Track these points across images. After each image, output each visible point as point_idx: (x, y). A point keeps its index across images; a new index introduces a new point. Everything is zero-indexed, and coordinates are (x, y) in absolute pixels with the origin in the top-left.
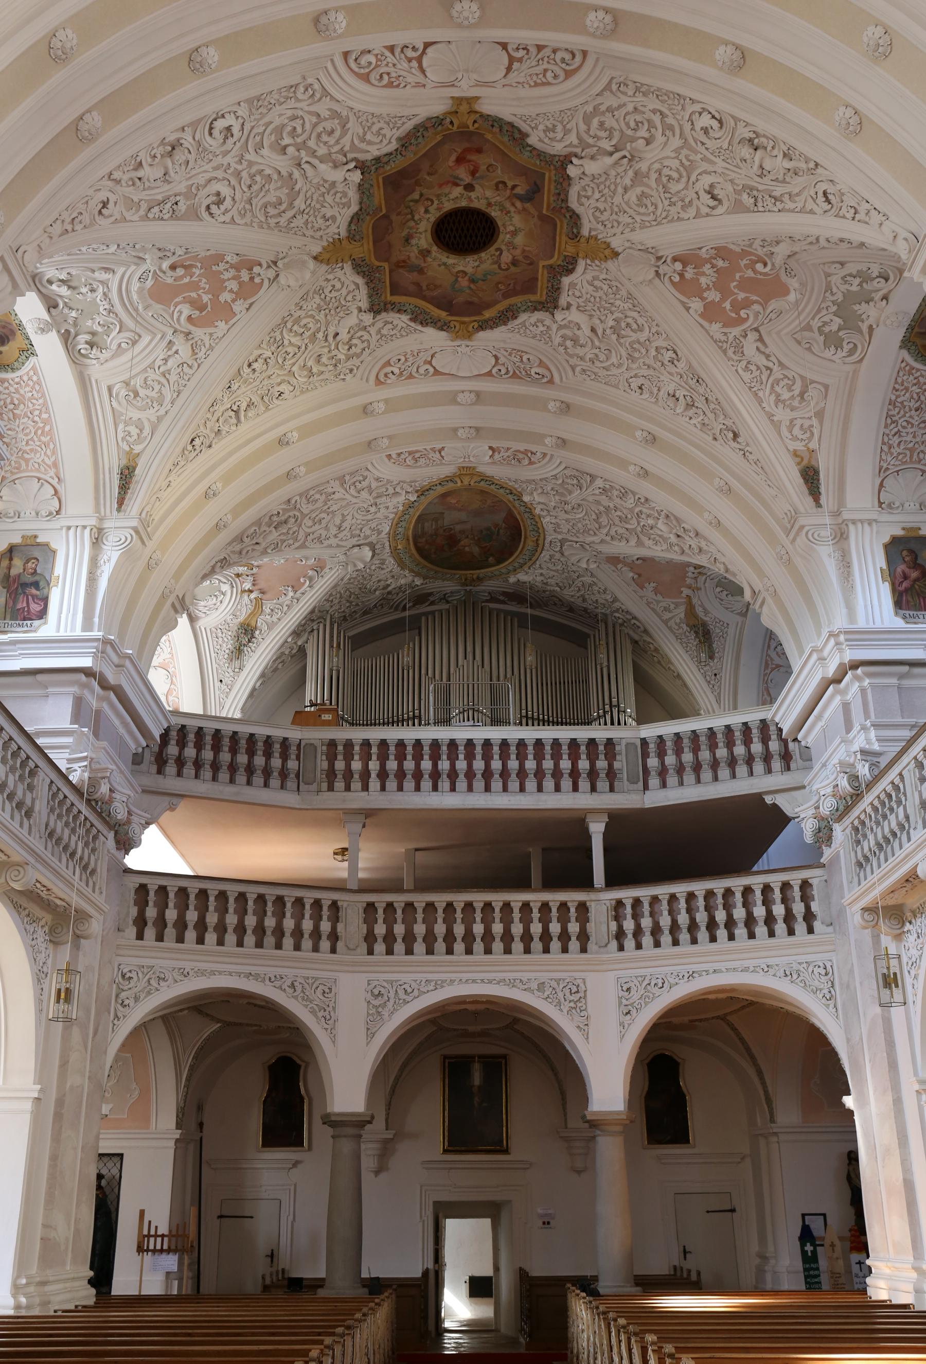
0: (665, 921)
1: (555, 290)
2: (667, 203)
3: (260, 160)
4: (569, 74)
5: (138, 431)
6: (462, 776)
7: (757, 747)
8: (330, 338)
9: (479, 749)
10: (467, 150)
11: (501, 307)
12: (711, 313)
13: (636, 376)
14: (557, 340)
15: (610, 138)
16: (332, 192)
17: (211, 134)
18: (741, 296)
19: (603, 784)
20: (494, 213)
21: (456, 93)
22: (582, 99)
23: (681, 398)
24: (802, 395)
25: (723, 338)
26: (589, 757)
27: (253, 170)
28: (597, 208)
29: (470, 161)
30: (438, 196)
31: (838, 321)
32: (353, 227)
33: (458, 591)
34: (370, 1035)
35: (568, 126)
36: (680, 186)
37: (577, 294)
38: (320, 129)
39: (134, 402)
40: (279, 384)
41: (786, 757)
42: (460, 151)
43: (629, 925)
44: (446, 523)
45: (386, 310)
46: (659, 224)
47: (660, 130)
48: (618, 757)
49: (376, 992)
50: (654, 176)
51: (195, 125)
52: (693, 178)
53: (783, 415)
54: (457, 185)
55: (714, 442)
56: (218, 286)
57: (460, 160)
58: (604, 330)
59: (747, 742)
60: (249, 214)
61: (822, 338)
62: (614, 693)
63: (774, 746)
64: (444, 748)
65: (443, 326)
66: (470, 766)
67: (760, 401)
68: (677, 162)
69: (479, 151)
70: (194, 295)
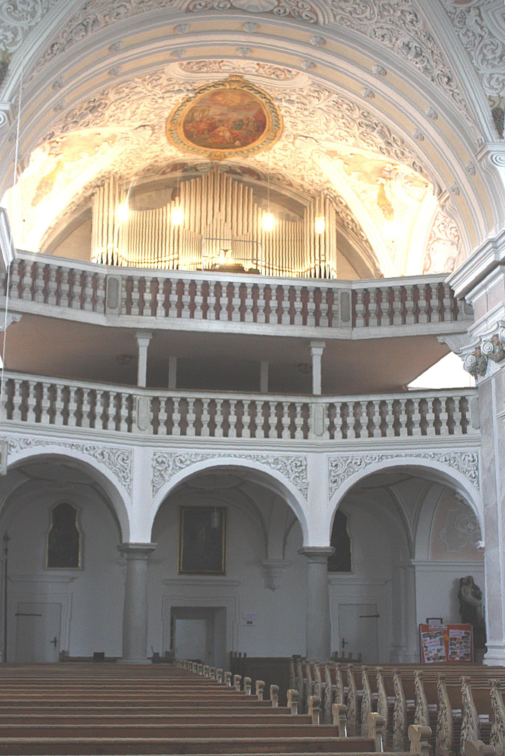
0: (364, 420)
5: (12, 36)
6: (224, 309)
7: (434, 302)
9: (237, 290)
13: (382, 28)
19: (324, 321)
23: (413, 49)
26: (315, 301)
33: (207, 164)
34: (155, 491)
39: (13, 14)
40: (118, 7)
41: (455, 311)
43: (338, 421)
44: (211, 113)
48: (335, 302)
49: (160, 460)
55: (432, 83)
59: (428, 298)
62: (322, 252)
63: (447, 302)
64: (212, 288)
66: (230, 302)
67: (471, 58)
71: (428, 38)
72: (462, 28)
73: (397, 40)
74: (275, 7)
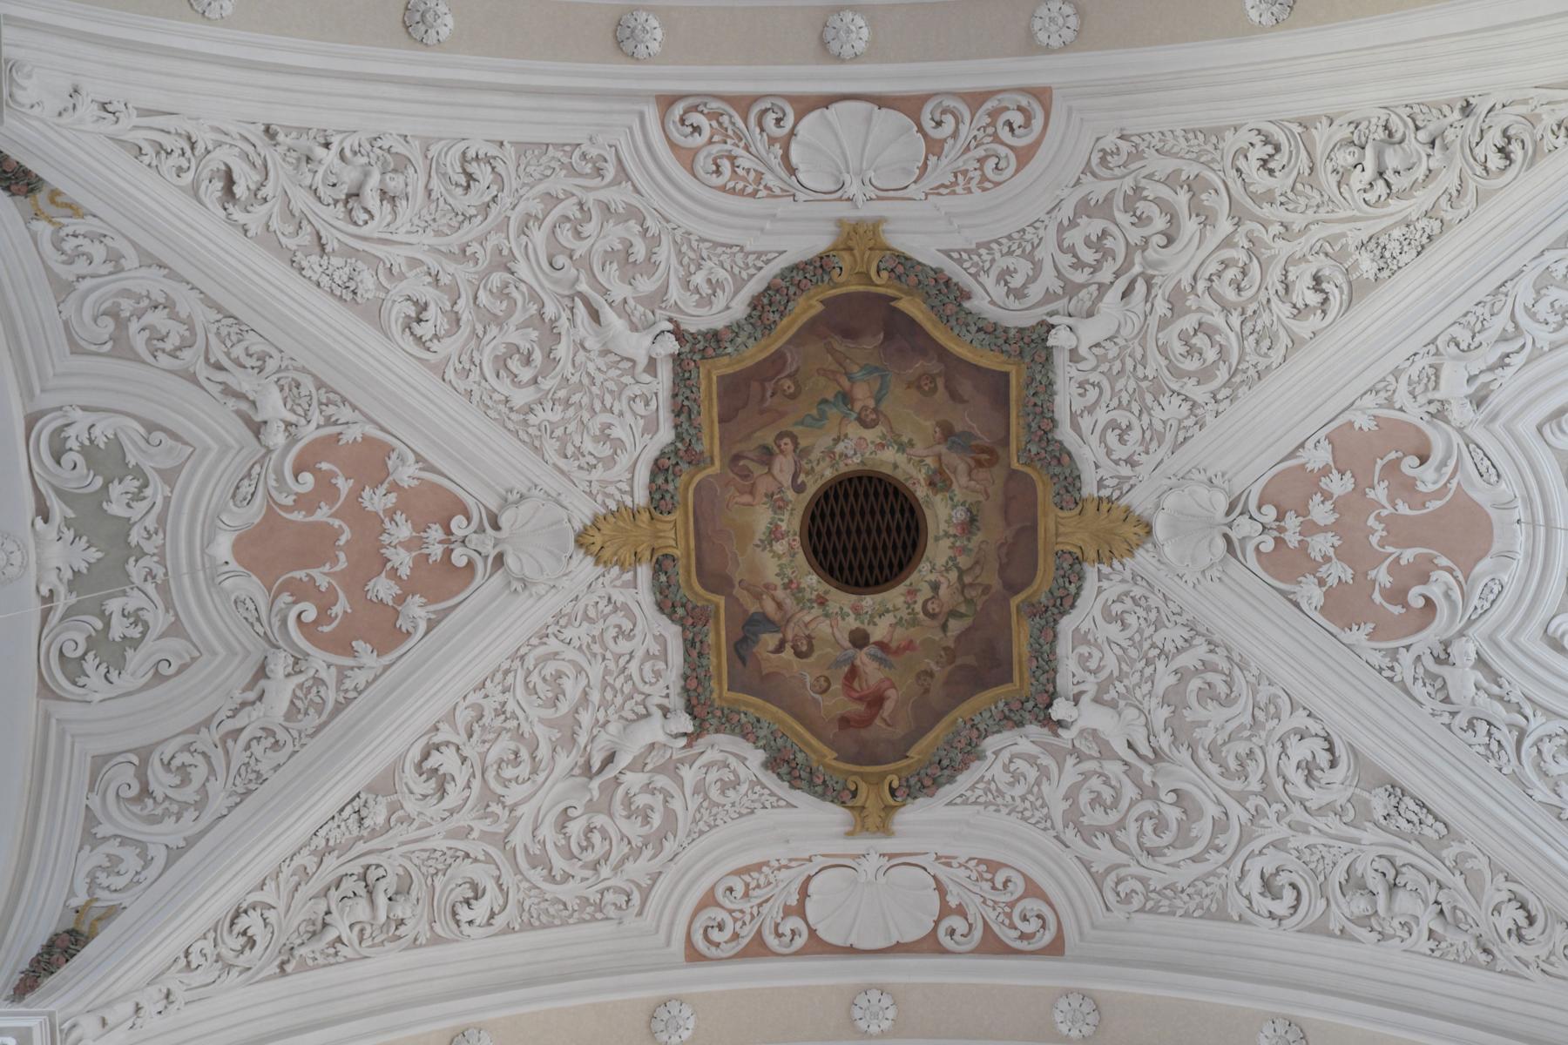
1: (681, 411)
2: (511, 706)
3: (1224, 797)
4: (709, 900)
8: (1140, 287)
10: (865, 722)
11: (788, 327)
12: (372, 461)
14: (665, 252)
15: (628, 801)
16: (1104, 675)
17: (1298, 898)
18: (322, 514)
20: (812, 581)
21: (888, 845)
22: (682, 860)
24: (122, 324)
25: (331, 410)
27: (1236, 785)
28: (629, 636)
29: (860, 699)
30: (914, 622)
31: (116, 508)
32: (1072, 588)
35: (699, 799)
36: (492, 757)
37: (639, 407)
38: (1114, 816)
40: (1268, 197)
42: (878, 722)
45: (1021, 330)
46: (512, 658)
47: (549, 846)
50: (544, 752)
51: (1319, 928)
52: (476, 784)
53: (151, 283)
54: (882, 645)
56: (1351, 510)
57: (876, 701)
58: (572, 321)
60: (1262, 699)
61: (132, 460)
65: (903, 266)
68: (509, 801)
69: (845, 722)
70: (1403, 509)
71: (354, 293)
72: (279, 370)
73: (429, 193)
74: (792, 133)
